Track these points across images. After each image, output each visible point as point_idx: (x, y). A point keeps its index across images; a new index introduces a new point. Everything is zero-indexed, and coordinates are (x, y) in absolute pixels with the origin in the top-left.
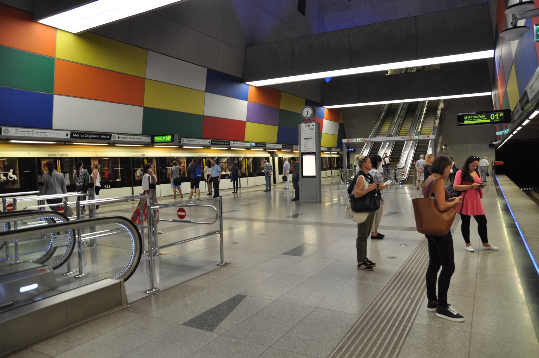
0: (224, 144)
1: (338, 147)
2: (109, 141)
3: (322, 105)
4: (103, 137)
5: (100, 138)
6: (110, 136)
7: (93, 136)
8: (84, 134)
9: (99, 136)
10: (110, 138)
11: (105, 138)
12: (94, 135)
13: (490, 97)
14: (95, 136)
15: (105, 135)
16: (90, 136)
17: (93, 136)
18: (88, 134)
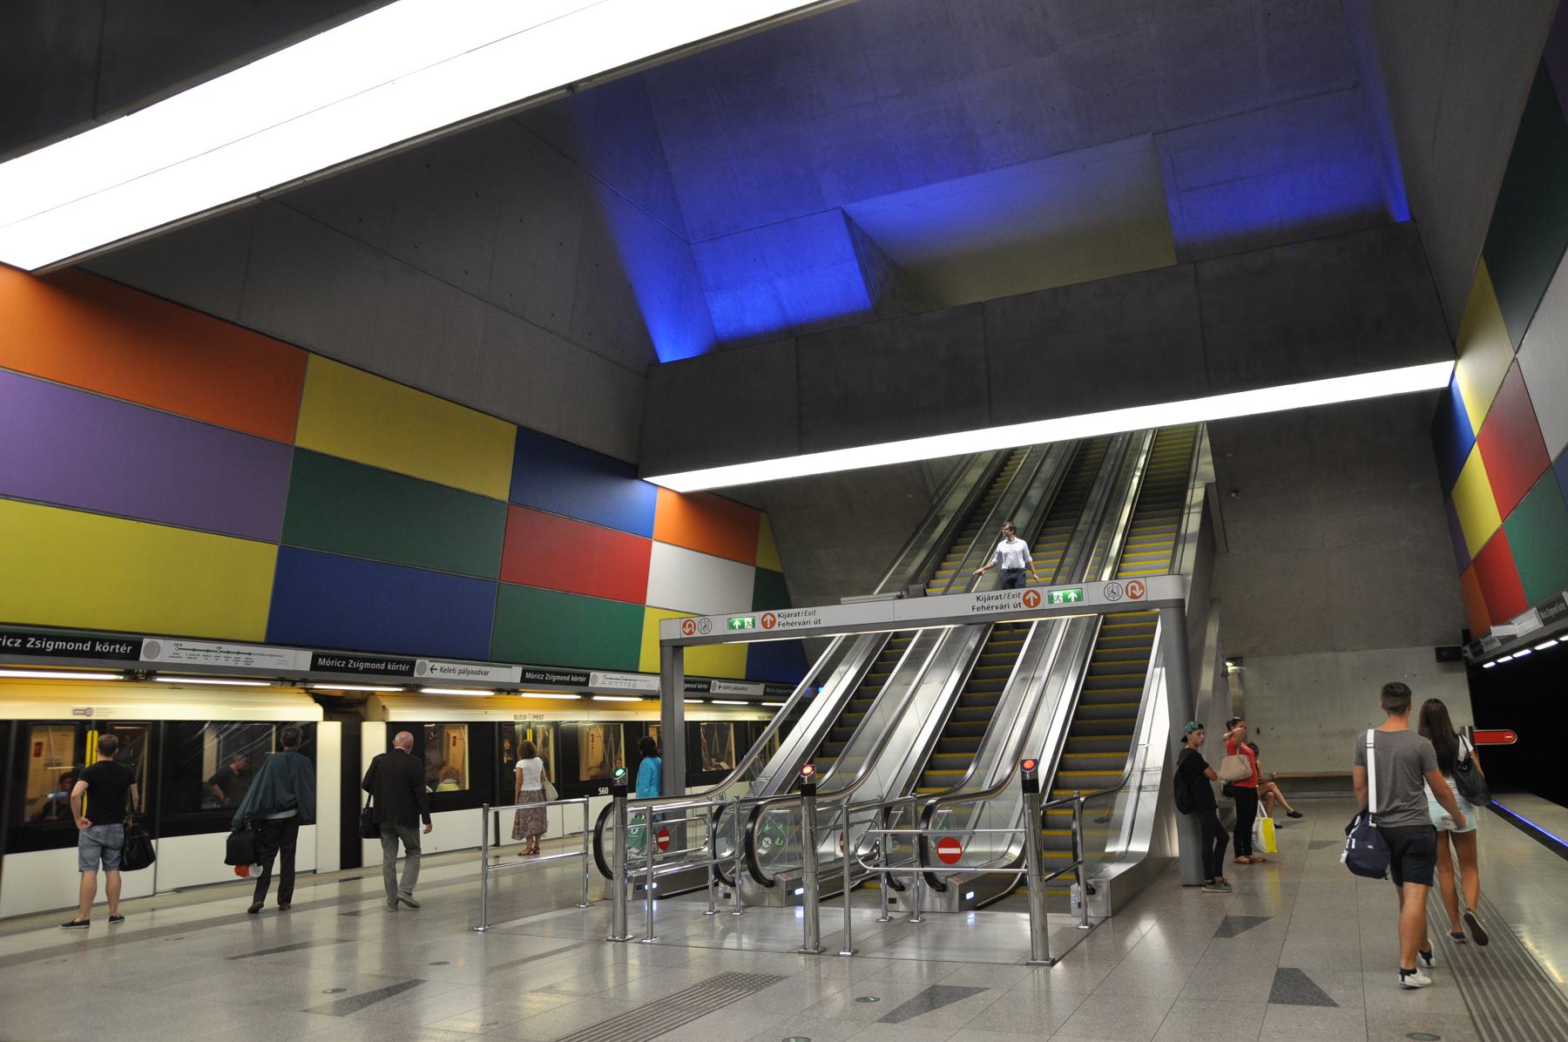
0: (386, 672)
1: (750, 678)
2: (129, 665)
3: (635, 471)
4: (106, 648)
5: (92, 654)
6: (136, 646)
7: (61, 645)
8: (25, 637)
9: (87, 647)
10: (135, 655)
11: (123, 654)
12: (67, 639)
13: (1444, 399)
14: (71, 646)
15: (112, 642)
16: (50, 646)
17: (61, 645)
18: (39, 637)
